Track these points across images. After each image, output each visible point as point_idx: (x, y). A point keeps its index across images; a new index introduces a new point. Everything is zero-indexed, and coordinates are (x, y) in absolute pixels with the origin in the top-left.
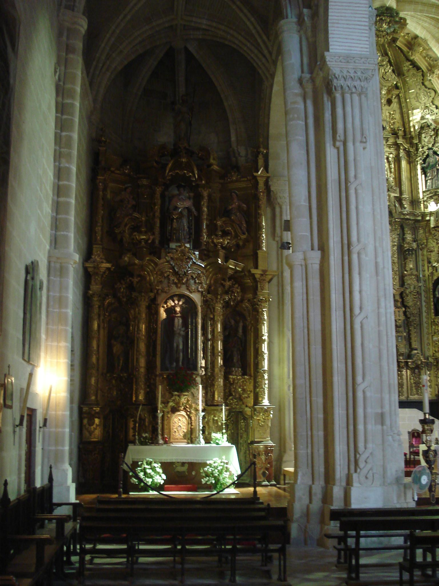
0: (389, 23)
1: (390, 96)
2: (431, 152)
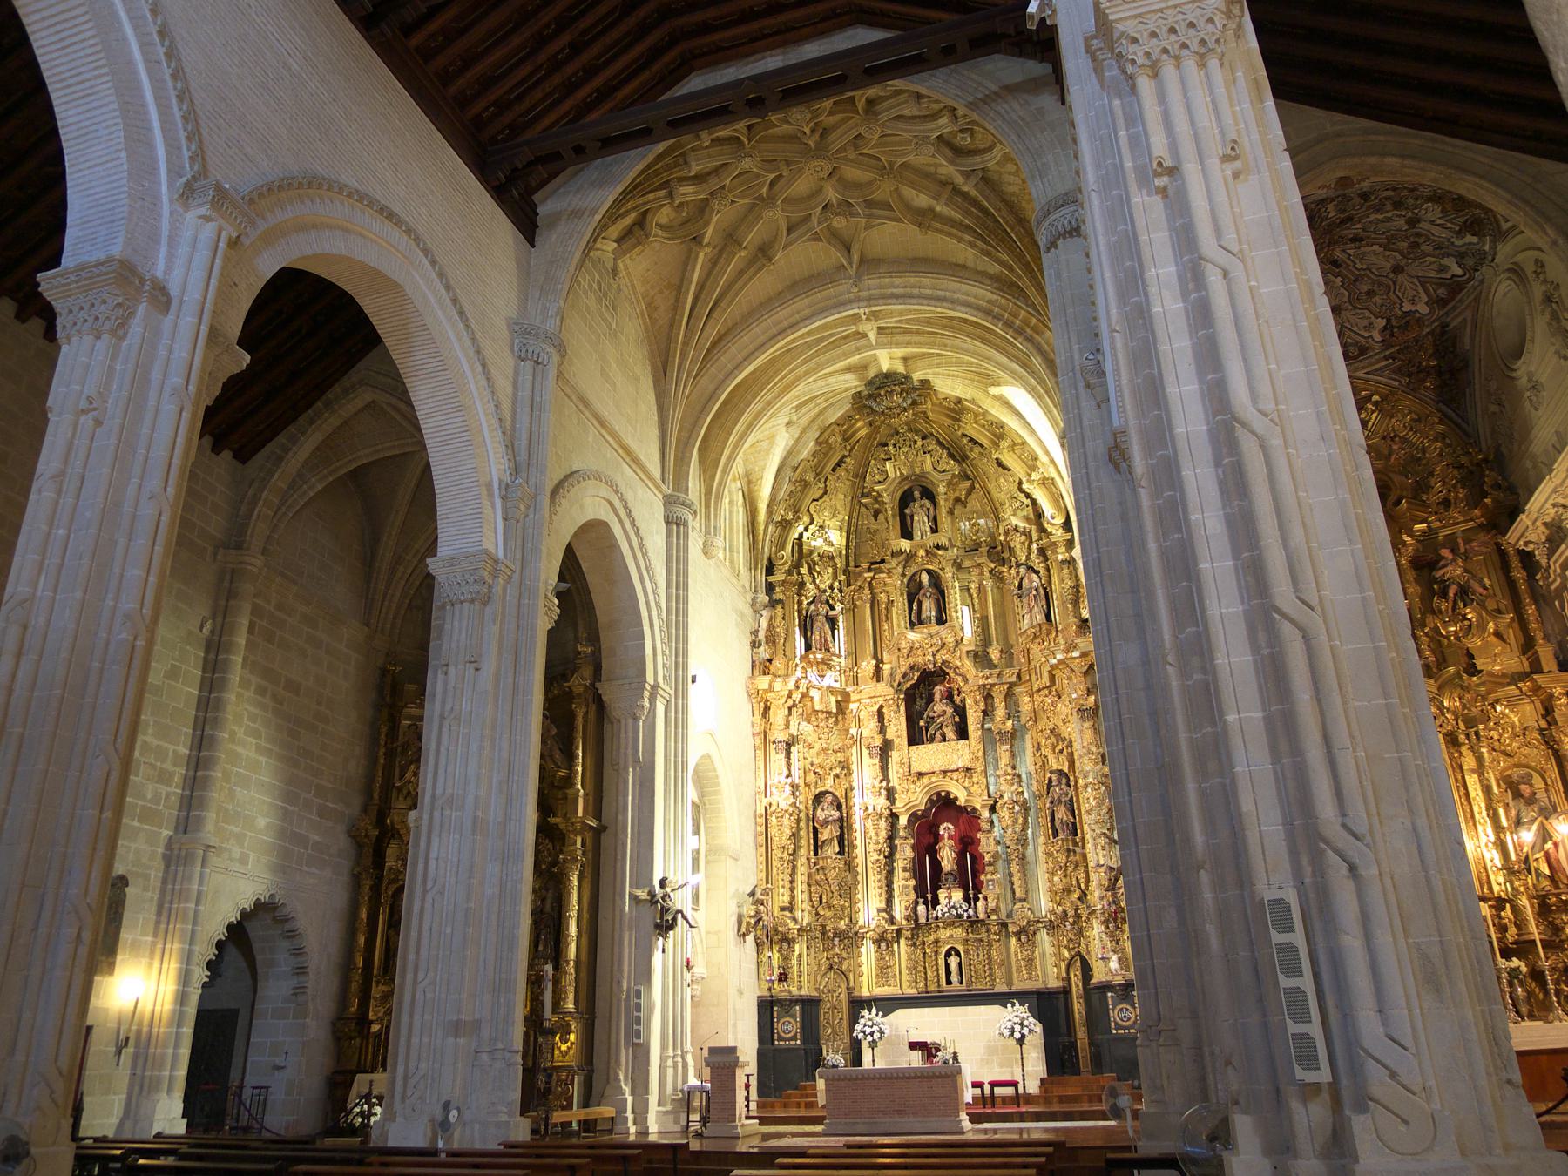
0: (901, 394)
1: (957, 494)
2: (1022, 570)
